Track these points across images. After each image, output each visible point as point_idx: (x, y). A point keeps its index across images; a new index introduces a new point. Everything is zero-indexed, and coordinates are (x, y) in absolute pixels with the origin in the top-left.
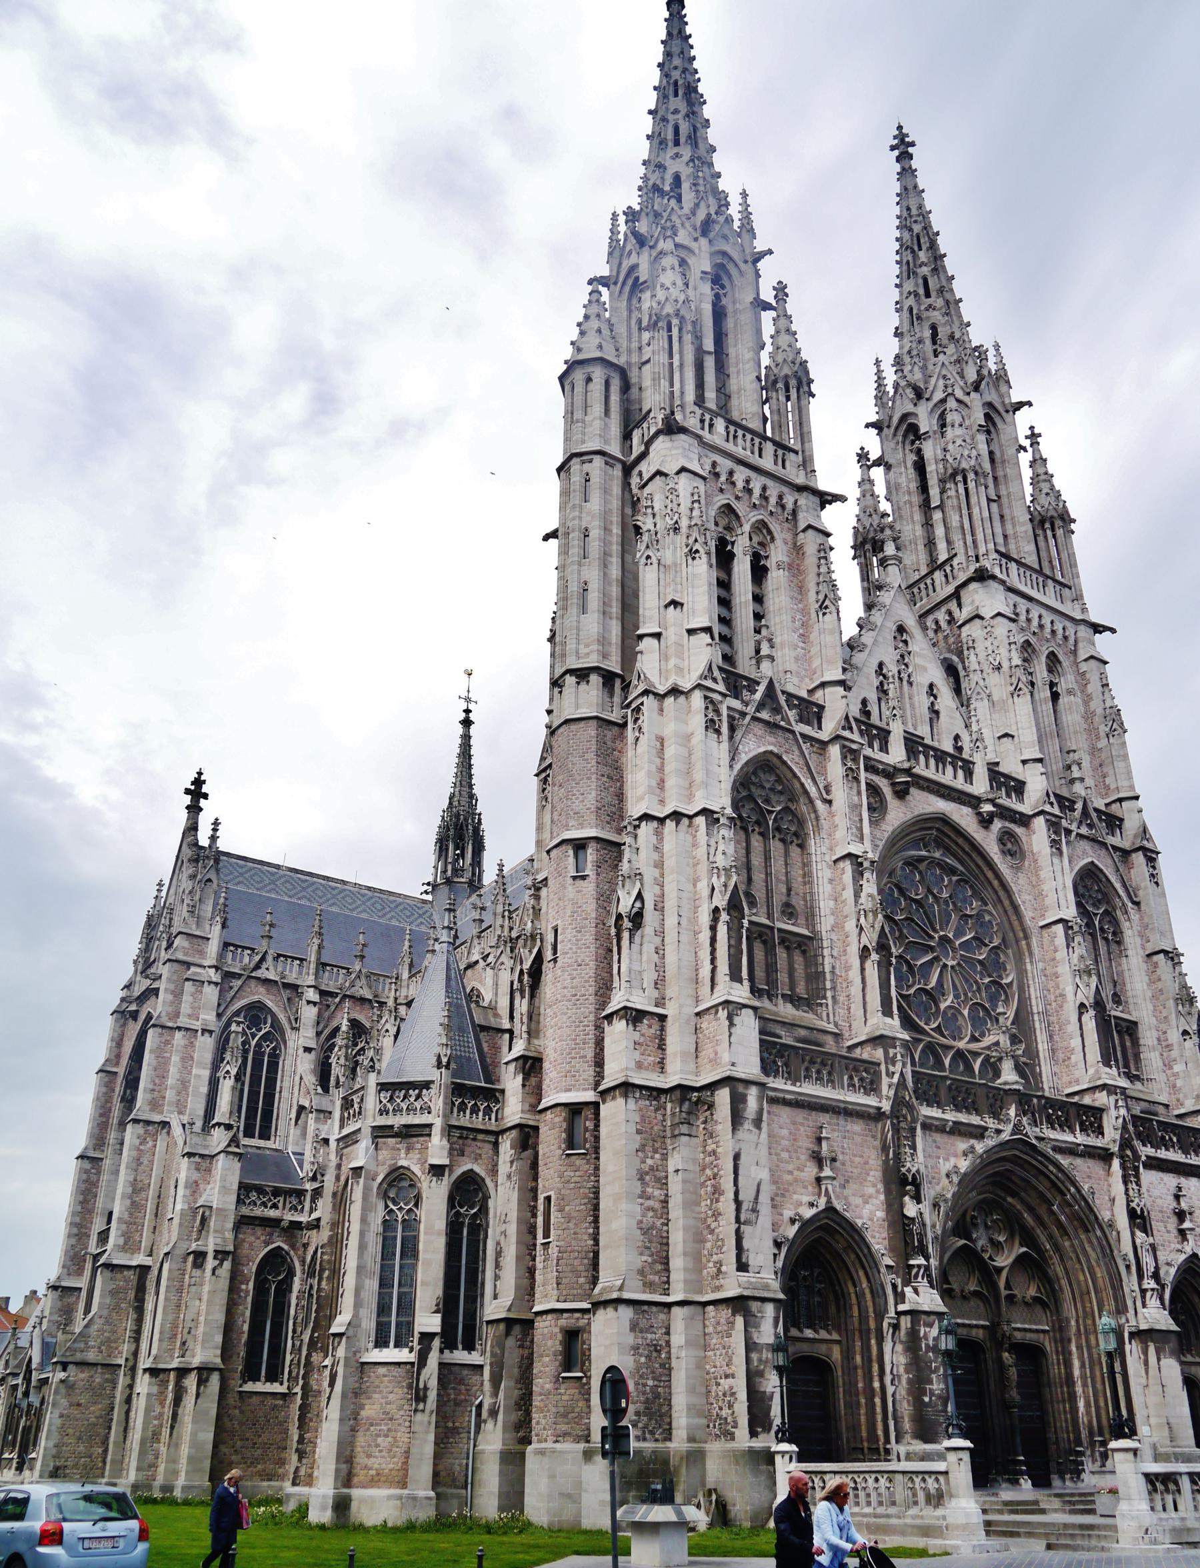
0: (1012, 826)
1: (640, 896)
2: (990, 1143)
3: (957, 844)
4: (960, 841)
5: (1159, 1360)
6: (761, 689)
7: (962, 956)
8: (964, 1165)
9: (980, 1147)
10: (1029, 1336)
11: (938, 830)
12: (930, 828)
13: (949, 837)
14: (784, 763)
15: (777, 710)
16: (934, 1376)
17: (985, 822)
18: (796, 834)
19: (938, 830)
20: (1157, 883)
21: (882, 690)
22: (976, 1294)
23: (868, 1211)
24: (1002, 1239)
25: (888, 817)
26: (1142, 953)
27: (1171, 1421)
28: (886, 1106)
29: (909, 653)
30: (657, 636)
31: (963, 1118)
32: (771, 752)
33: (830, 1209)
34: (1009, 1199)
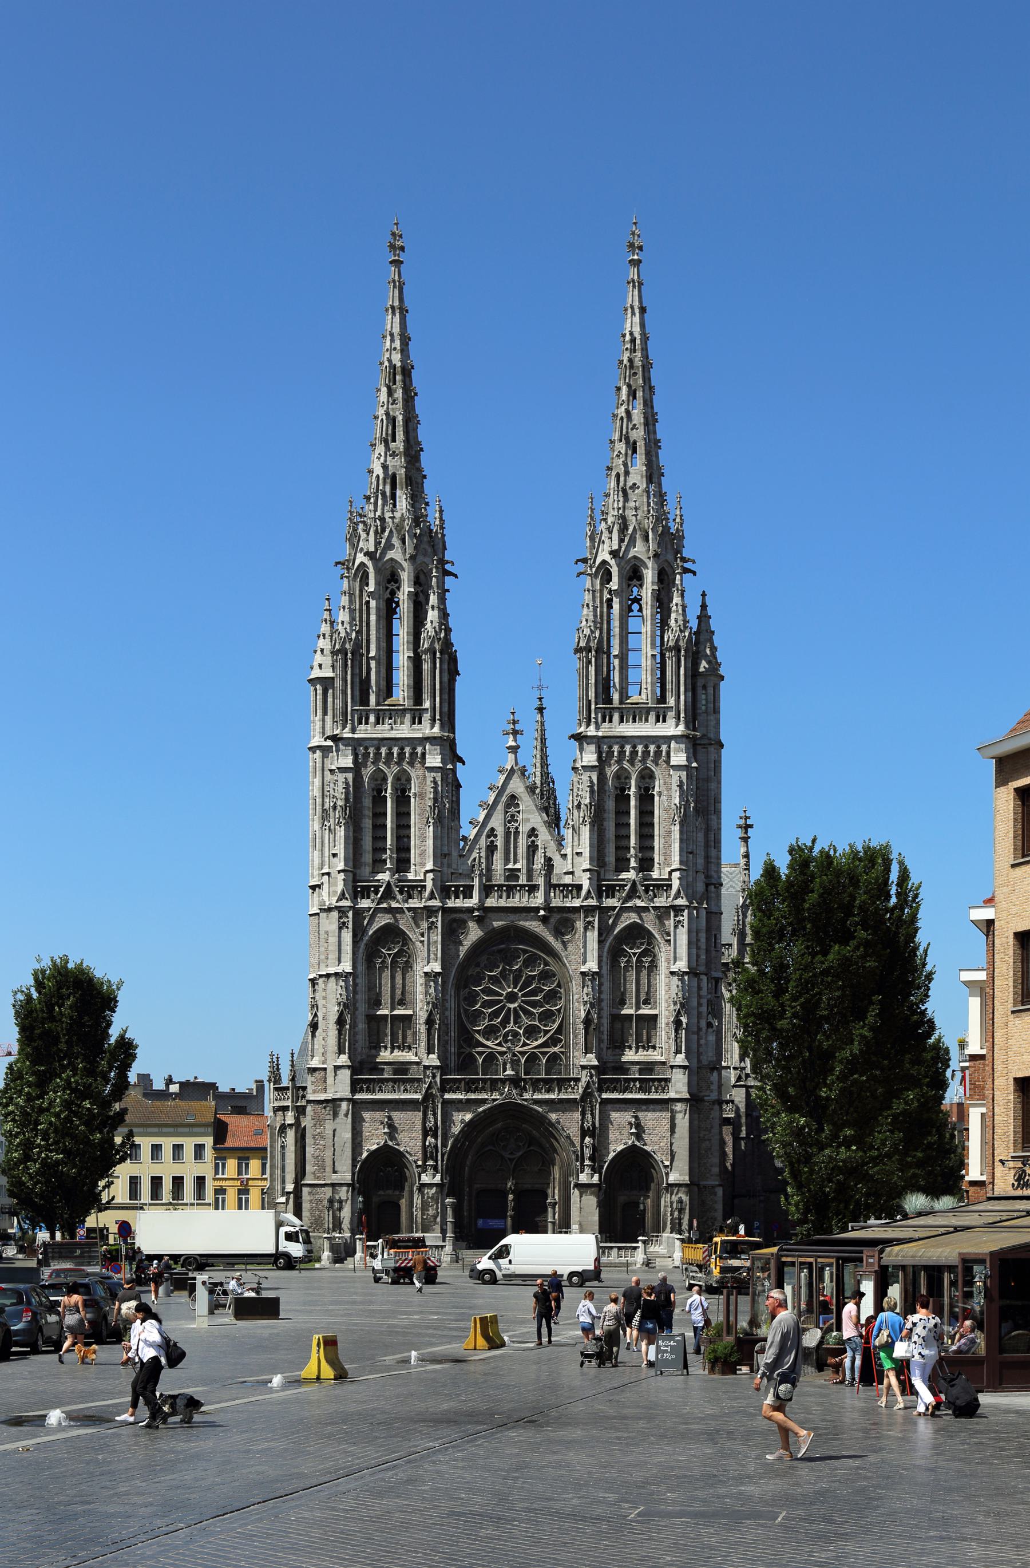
0: (569, 915)
1: (316, 1015)
5: (581, 1197)
6: (382, 889)
7: (522, 1001)
8: (468, 1117)
15: (394, 898)
17: (544, 920)
18: (407, 962)
21: (491, 849)
23: (410, 1143)
26: (667, 972)
28: (420, 1097)
29: (519, 812)
30: (328, 874)
31: (473, 1096)
33: (386, 1145)
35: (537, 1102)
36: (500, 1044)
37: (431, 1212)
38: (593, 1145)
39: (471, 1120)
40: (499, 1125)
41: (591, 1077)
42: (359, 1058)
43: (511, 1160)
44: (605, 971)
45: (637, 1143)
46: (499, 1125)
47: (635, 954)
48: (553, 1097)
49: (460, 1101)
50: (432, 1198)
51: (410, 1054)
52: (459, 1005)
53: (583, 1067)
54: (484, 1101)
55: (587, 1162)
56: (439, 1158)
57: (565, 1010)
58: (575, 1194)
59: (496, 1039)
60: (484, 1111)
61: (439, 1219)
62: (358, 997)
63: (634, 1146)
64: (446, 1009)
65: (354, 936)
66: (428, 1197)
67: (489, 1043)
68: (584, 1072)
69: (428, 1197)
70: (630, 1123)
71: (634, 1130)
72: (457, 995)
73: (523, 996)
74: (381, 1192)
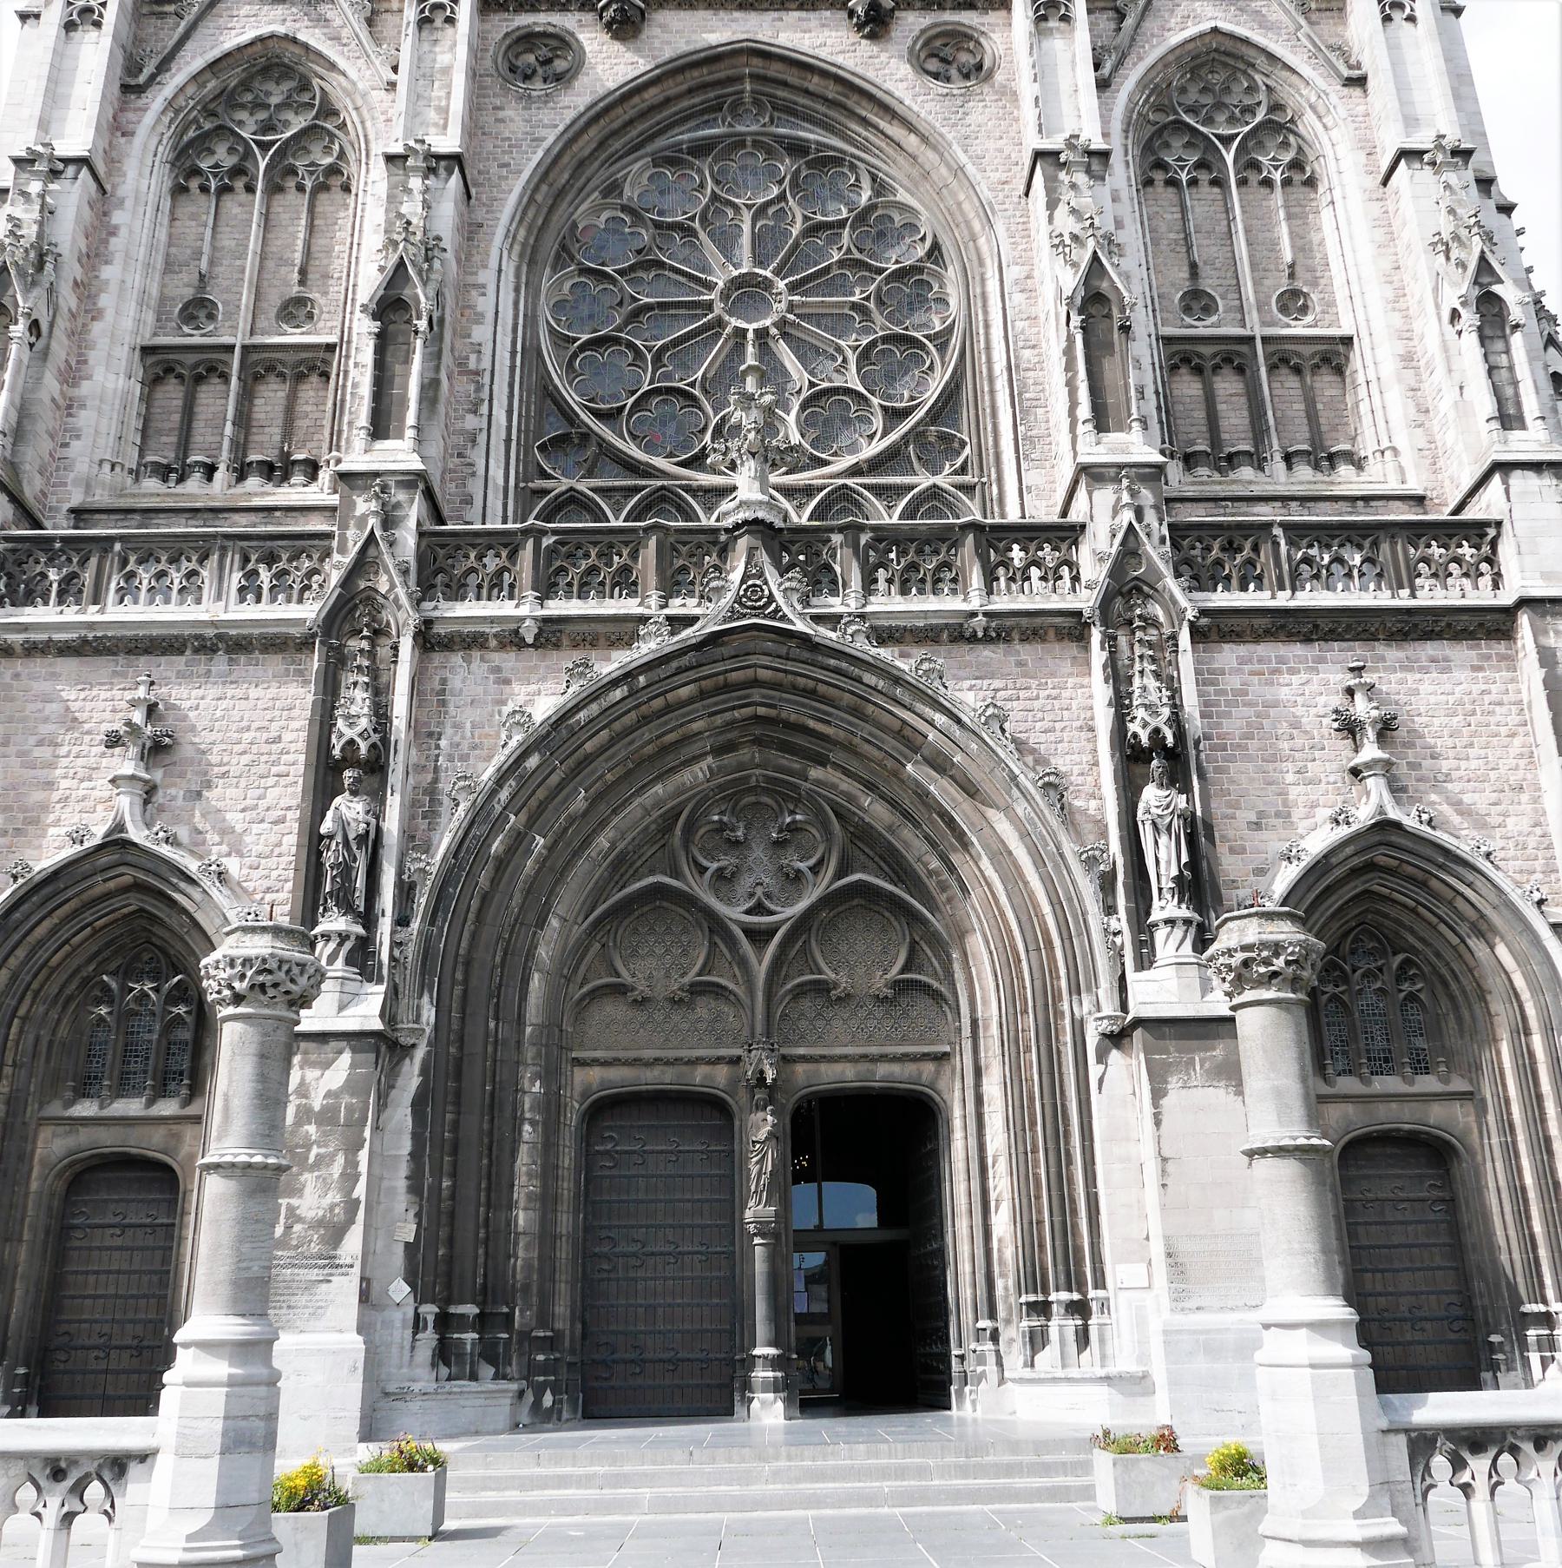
2: (648, 647)
3: (807, 92)
4: (814, 84)
5: (1158, 1094)
9: (610, 664)
10: (883, 1070)
11: (754, 77)
12: (739, 79)
13: (785, 84)
14: (306, 47)
16: (308, 1178)
18: (333, 170)
19: (754, 77)
20: (1411, 19)
22: (698, 990)
24: (802, 866)
25: (582, 82)
27: (1183, 1246)
32: (272, 36)
33: (116, 842)
34: (816, 773)
35: (884, 636)
36: (697, 462)
37: (313, 1198)
38: (1189, 819)
39: (562, 718)
40: (698, 773)
41: (1139, 513)
42: (76, 499)
43: (760, 937)
44: (1121, 173)
45: (1393, 814)
46: (698, 773)
47: (1227, 140)
48: (954, 604)
49: (512, 639)
50: (326, 1117)
51: (313, 487)
52: (531, 320)
53: (1091, 474)
54: (624, 631)
55: (1165, 907)
56: (387, 898)
57: (969, 333)
58: (1120, 1082)
59: (686, 447)
60: (628, 676)
61: (353, 1244)
62: (108, 272)
63: (1385, 827)
64: (479, 318)
65: (132, 66)
66: (305, 1114)
67: (660, 462)
68: (1105, 496)
69: (305, 1114)
70: (1350, 728)
71: (1370, 751)
72: (528, 285)
73: (792, 288)
74: (86, 1108)
